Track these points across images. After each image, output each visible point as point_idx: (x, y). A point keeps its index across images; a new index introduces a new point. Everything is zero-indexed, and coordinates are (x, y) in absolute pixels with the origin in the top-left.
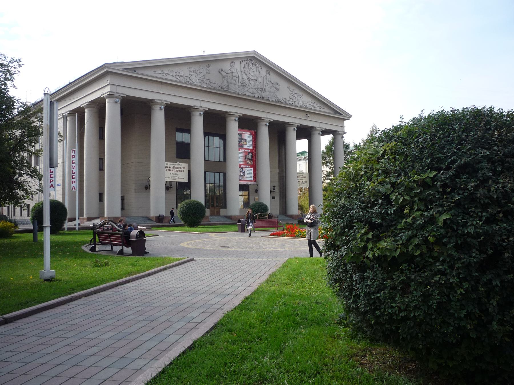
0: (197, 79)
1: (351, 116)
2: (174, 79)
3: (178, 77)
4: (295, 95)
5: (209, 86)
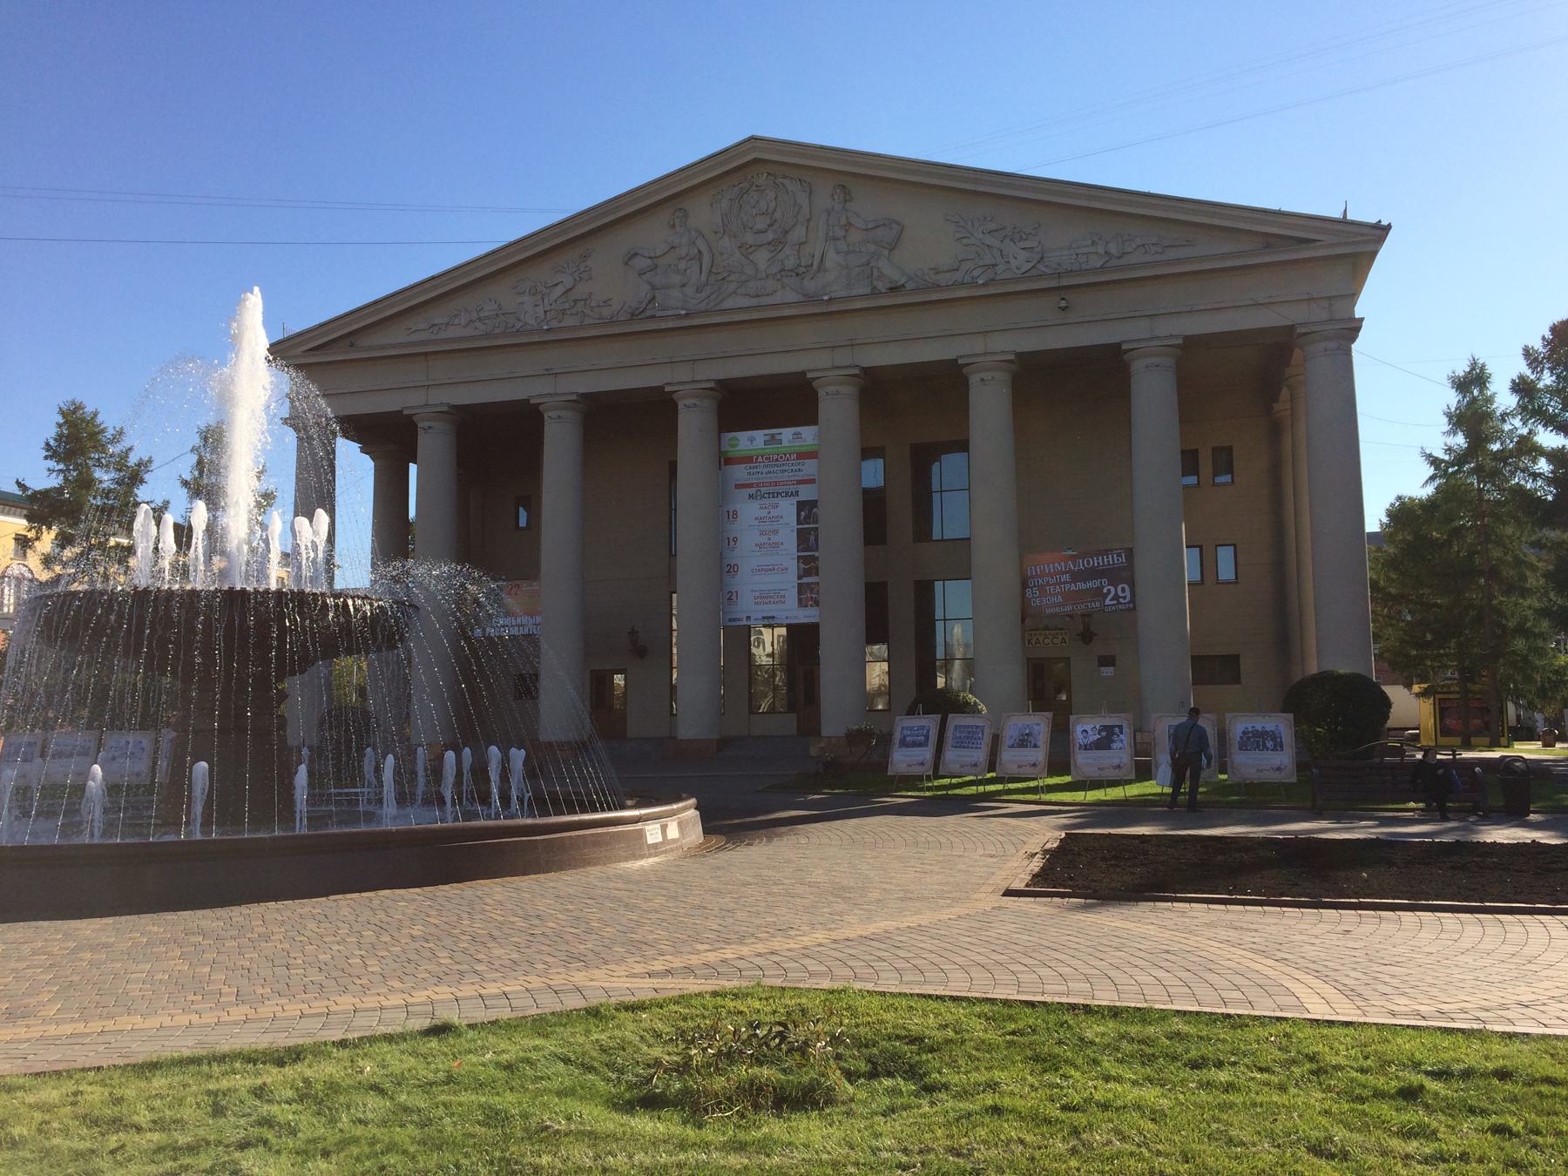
0: (540, 311)
1: (1380, 232)
2: (468, 332)
3: (478, 324)
4: (989, 240)
5: (588, 321)
